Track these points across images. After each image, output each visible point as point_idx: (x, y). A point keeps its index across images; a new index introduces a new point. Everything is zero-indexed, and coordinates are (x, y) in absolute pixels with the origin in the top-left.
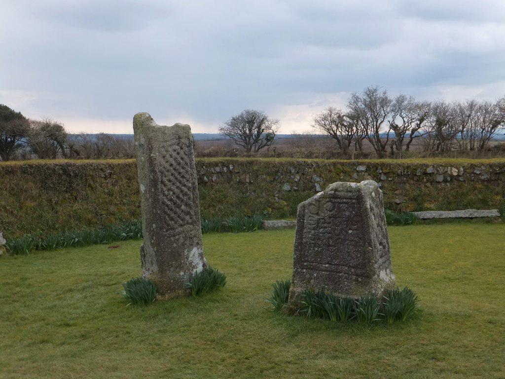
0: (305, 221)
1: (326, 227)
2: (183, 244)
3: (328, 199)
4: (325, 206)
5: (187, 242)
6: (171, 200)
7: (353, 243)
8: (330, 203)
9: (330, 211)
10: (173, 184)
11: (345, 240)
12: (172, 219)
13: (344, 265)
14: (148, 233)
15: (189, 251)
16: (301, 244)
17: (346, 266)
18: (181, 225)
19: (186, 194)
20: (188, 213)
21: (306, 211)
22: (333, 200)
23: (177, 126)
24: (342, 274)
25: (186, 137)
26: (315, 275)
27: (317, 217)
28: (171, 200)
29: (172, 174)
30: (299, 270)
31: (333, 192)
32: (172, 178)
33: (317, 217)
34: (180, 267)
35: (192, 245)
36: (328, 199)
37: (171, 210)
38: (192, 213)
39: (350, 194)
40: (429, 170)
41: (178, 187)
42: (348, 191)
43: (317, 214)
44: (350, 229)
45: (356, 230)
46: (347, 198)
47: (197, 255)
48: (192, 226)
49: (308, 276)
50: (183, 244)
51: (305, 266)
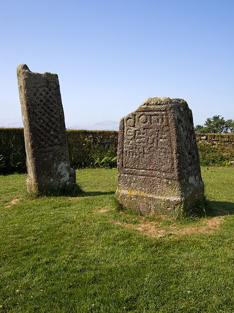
1: (140, 138)
2: (53, 159)
5: (56, 158)
6: (41, 126)
7: (163, 150)
9: (144, 123)
10: (43, 115)
11: (157, 148)
12: (43, 140)
13: (157, 170)
15: (58, 165)
18: (50, 146)
19: (54, 123)
20: (57, 137)
22: (146, 113)
23: (48, 74)
24: (156, 178)
25: (53, 82)
26: (134, 179)
27: (133, 129)
28: (41, 126)
29: (42, 108)
30: (122, 175)
32: (42, 110)
33: (133, 129)
34: (50, 175)
35: (60, 160)
37: (42, 133)
38: (60, 137)
41: (47, 118)
42: (157, 104)
43: (134, 126)
44: (161, 138)
47: (64, 168)
48: (59, 147)
50: (53, 159)
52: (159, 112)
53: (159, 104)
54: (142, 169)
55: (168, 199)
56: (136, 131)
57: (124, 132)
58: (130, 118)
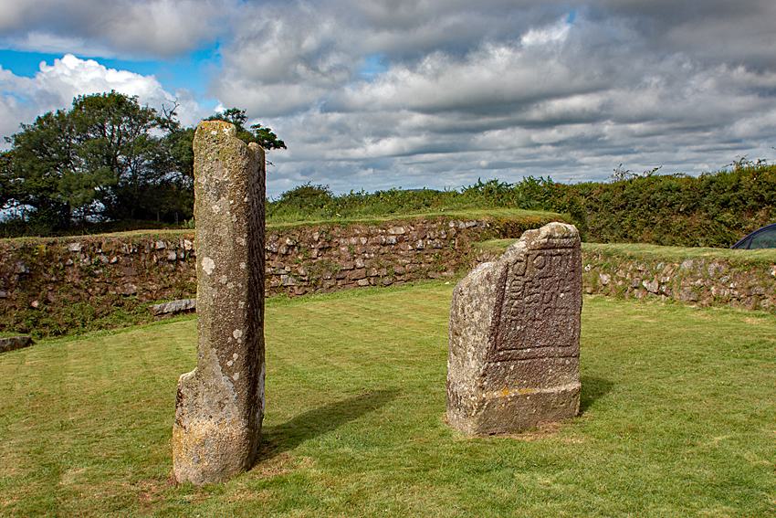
0: (507, 288)
7: (563, 311)
14: (215, 350)
16: (498, 324)
21: (510, 272)
22: (545, 252)
26: (512, 368)
36: (538, 252)
40: (160, 245)
46: (561, 248)
52: (564, 250)
53: (566, 238)
54: (526, 349)
55: (563, 389)
57: (505, 286)
58: (521, 261)
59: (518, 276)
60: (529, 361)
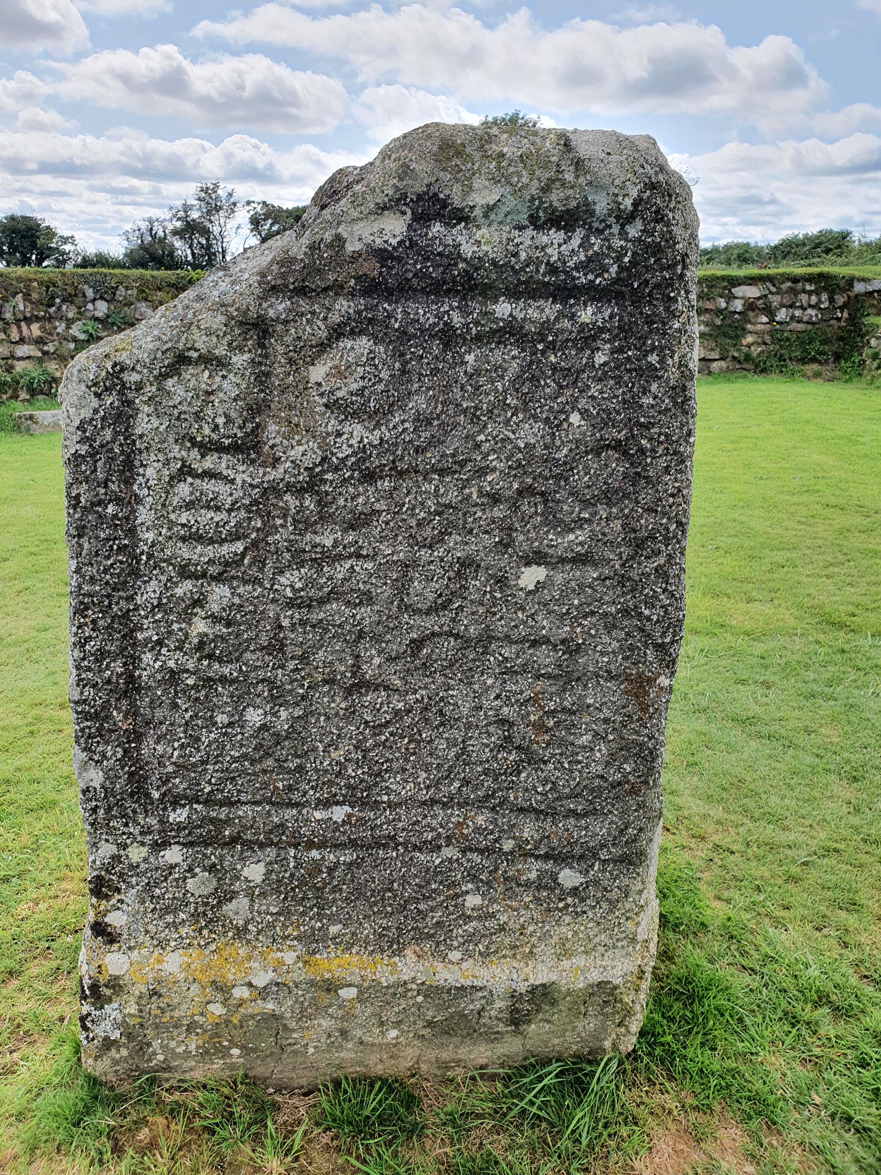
0: (144, 515)
3: (343, 306)
4: (318, 372)
8: (364, 344)
9: (377, 417)
17: (482, 803)
26: (255, 872)
31: (394, 228)
36: (343, 306)
39: (557, 245)
43: (247, 447)
45: (581, 560)
49: (199, 885)
51: (180, 827)
52: (539, 312)
56: (272, 490)
59: (205, 448)
60: (347, 856)
